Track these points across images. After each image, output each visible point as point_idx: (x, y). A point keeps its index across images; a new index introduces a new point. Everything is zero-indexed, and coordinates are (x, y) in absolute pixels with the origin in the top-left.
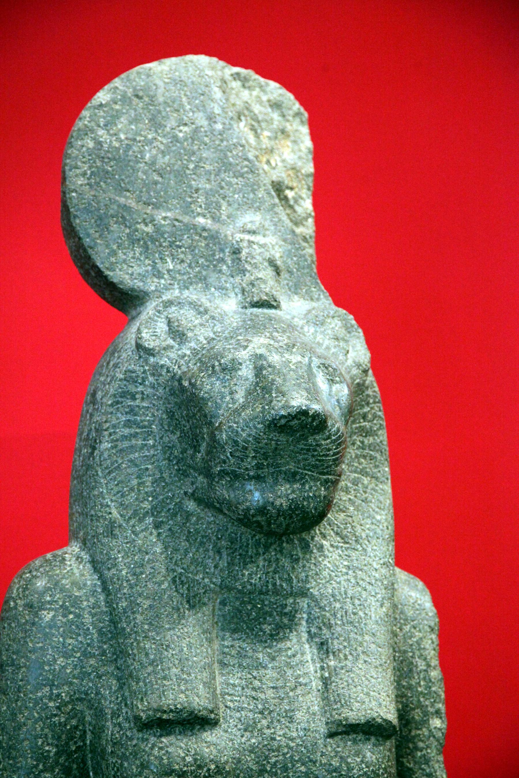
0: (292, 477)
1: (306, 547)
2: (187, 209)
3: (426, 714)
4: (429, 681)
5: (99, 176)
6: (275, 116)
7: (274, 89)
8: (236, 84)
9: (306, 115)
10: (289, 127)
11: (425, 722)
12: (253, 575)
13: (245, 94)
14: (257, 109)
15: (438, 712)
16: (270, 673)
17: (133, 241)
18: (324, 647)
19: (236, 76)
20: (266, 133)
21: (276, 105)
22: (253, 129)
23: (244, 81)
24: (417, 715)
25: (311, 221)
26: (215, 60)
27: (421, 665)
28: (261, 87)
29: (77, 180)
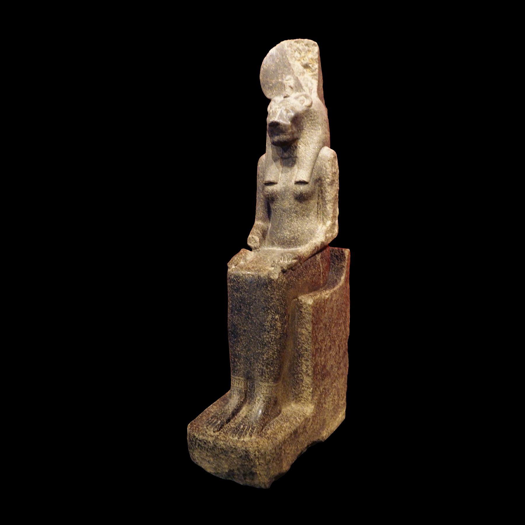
0: (278, 135)
1: (296, 147)
2: (278, 78)
3: (325, 178)
4: (326, 172)
5: (264, 75)
6: (307, 48)
7: (306, 40)
8: (295, 44)
9: (316, 43)
10: (310, 49)
11: (325, 180)
12: (286, 155)
13: (298, 45)
14: (301, 48)
15: (328, 178)
16: (289, 173)
17: (269, 88)
18: (298, 168)
19: (296, 42)
20: (303, 53)
21: (307, 45)
22: (299, 53)
23: (297, 42)
24: (323, 179)
25: (317, 70)
26: (288, 40)
27: (324, 168)
28: (303, 42)
29: (261, 78)
